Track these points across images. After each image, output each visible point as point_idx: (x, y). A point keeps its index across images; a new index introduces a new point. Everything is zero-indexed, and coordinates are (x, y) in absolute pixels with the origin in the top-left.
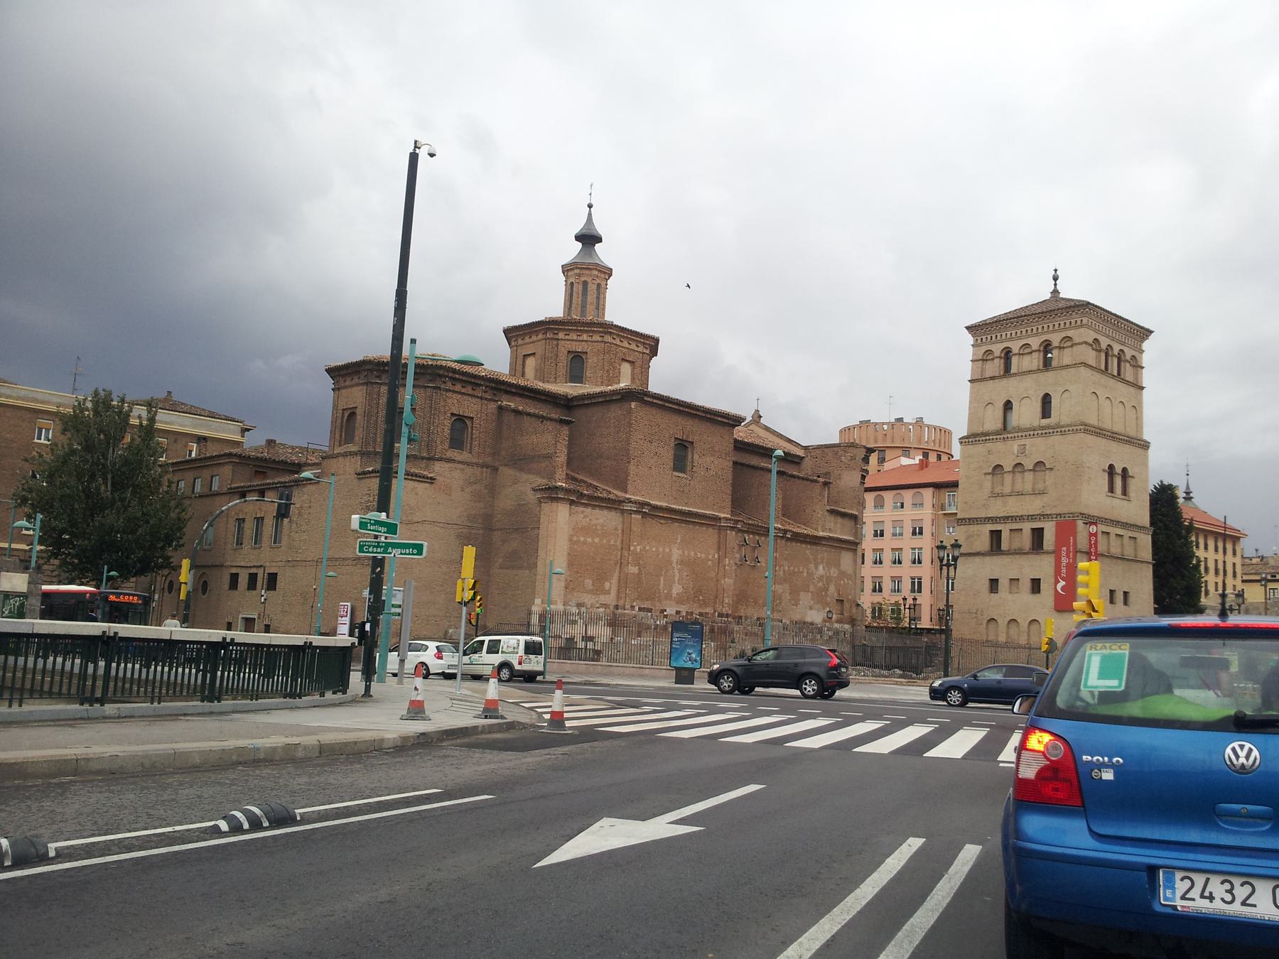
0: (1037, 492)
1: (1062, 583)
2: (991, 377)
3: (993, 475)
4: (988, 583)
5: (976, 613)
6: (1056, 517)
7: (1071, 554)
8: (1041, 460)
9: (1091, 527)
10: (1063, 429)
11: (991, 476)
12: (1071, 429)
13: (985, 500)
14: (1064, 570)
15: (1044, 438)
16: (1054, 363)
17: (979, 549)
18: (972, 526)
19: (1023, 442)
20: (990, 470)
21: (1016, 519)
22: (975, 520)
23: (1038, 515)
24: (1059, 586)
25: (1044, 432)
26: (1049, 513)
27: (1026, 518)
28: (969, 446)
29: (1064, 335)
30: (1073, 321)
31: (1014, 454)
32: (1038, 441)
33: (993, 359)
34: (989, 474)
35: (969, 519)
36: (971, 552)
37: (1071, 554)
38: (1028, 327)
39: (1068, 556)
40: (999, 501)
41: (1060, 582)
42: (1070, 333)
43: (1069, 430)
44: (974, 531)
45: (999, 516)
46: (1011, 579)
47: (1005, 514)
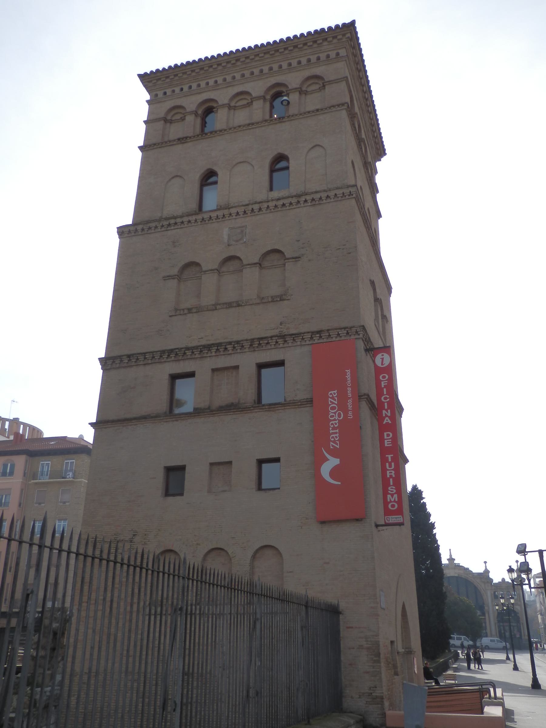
1: (333, 462)
2: (179, 139)
3: (179, 281)
4: (160, 475)
7: (350, 401)
8: (277, 247)
10: (317, 196)
11: (176, 280)
14: (335, 436)
16: (293, 110)
21: (226, 349)
24: (326, 470)
25: (280, 203)
27: (247, 345)
29: (307, 73)
33: (183, 119)
35: (129, 356)
36: (128, 416)
37: (350, 401)
39: (342, 406)
41: (327, 460)
42: (317, 71)
45: (190, 345)
46: (212, 464)
47: (204, 342)
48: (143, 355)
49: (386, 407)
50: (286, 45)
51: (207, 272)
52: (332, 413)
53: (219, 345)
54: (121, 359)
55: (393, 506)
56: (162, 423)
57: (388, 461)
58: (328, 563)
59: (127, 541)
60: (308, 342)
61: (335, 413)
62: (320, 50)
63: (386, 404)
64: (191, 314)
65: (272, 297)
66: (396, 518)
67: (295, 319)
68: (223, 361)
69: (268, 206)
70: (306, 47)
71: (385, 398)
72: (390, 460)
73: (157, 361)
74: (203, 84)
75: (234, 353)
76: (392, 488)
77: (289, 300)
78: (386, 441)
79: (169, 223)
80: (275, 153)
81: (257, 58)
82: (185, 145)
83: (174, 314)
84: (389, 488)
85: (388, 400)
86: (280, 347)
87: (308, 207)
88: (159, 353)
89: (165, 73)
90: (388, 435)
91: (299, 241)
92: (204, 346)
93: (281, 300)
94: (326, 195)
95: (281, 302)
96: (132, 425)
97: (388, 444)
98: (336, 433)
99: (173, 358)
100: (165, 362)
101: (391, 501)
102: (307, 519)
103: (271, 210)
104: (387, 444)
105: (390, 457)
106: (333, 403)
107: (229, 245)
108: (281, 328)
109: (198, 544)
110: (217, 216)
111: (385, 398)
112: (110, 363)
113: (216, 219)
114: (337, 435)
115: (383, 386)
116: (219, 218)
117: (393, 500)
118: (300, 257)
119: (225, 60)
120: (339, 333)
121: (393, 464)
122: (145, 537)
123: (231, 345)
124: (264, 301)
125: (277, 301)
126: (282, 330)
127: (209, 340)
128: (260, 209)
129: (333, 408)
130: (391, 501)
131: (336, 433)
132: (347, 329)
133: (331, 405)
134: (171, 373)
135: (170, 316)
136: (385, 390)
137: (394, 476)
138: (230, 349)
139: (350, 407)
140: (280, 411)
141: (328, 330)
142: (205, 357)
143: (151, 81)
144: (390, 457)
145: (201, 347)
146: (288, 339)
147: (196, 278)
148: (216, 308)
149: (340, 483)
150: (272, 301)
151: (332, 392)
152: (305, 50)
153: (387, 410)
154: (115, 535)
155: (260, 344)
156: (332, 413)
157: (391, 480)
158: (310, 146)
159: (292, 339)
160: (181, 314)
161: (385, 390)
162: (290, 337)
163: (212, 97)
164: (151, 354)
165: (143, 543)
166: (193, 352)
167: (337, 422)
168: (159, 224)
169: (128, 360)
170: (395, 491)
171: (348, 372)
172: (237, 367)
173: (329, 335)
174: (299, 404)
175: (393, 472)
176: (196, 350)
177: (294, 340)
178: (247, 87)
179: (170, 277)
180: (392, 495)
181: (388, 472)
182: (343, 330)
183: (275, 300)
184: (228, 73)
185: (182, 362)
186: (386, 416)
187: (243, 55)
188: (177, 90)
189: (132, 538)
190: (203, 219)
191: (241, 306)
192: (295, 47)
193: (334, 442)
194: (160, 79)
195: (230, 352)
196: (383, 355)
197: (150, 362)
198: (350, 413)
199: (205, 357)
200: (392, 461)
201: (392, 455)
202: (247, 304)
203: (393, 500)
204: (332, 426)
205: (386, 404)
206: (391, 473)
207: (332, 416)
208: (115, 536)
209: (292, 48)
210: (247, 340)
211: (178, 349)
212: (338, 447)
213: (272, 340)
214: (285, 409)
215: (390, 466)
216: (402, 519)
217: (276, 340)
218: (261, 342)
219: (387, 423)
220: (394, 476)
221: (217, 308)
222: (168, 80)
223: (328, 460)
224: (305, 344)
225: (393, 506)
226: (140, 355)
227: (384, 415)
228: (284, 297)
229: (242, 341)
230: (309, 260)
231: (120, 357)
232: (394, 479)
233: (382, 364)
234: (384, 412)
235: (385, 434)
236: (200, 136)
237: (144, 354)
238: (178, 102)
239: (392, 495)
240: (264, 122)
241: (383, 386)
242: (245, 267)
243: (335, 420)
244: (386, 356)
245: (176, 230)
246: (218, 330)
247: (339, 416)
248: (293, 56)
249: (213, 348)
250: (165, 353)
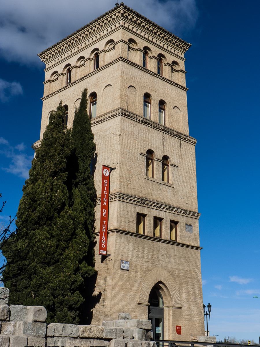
9: (105, 170)
49: (105, 197)
55: (103, 246)
71: (105, 192)
72: (104, 224)
84: (103, 237)
85: (106, 194)
90: (105, 211)
101: (103, 244)
104: (104, 215)
105: (104, 222)
111: (105, 192)
121: (105, 225)
130: (103, 244)
137: (105, 232)
144: (104, 222)
180: (104, 240)
181: (103, 229)
196: (106, 170)
206: (104, 230)
215: (104, 227)
216: (106, 253)
220: (105, 232)
225: (103, 246)
234: (104, 199)
235: (104, 210)
239: (104, 240)
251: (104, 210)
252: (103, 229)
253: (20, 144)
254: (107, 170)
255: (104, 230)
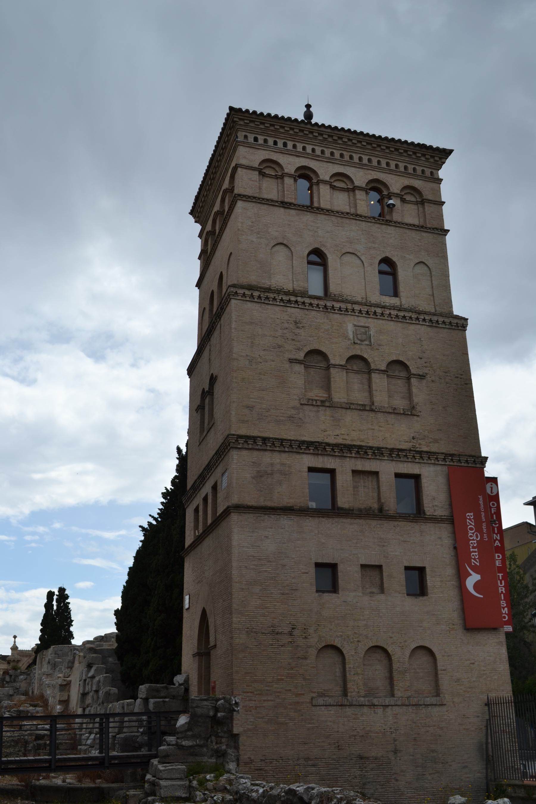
0: (402, 412)
5: (291, 634)
6: (444, 459)
8: (401, 359)
10: (435, 318)
12: (447, 320)
13: (293, 408)
14: (475, 554)
15: (400, 325)
16: (396, 217)
17: (286, 501)
18: (267, 453)
19: (363, 321)
20: (301, 356)
21: (366, 453)
22: (277, 444)
23: (410, 450)
25: (401, 314)
26: (425, 449)
28: (249, 305)
29: (407, 182)
30: (419, 169)
31: (346, 337)
32: (391, 326)
34: (299, 362)
36: (269, 504)
38: (345, 150)
39: (478, 529)
40: (325, 415)
43: (444, 322)
44: (272, 464)
46: (363, 566)
47: (340, 441)
48: (280, 441)
49: (496, 532)
50: (389, 144)
51: (336, 367)
52: (471, 533)
53: (360, 447)
54: (255, 440)
56: (307, 517)
57: (499, 579)
58: (473, 664)
59: (286, 633)
60: (440, 463)
61: (473, 533)
62: (417, 163)
63: (496, 529)
64: (324, 408)
65: (403, 410)
66: (507, 628)
67: (425, 436)
68: (361, 465)
69: (390, 313)
70: (405, 154)
71: (496, 524)
72: (501, 578)
73: (295, 450)
74: (300, 147)
75: (373, 459)
76: (503, 602)
77: (418, 416)
78: (497, 561)
79: (289, 299)
80: (383, 256)
81: (359, 145)
82: (287, 210)
83: (306, 403)
85: (497, 525)
86: (417, 461)
87: (426, 326)
88: (297, 442)
89: (261, 118)
90: (499, 557)
91: (421, 358)
92: (345, 446)
93: (411, 415)
94: (442, 320)
95: (411, 417)
96: (275, 514)
97: (499, 564)
98: (475, 552)
99: (311, 451)
100: (303, 453)
102: (453, 625)
103: (392, 318)
106: (471, 524)
107: (354, 343)
108: (414, 443)
109: (358, 641)
110: (340, 308)
112: (242, 442)
113: (338, 310)
114: (477, 554)
115: (493, 513)
116: (342, 311)
117: (504, 612)
118: (425, 376)
119: (328, 132)
120: (468, 459)
121: (503, 581)
122: (305, 631)
123: (372, 450)
124: (396, 411)
125: (408, 414)
126: (414, 444)
127: (346, 440)
128: (382, 314)
129: (471, 529)
131: (475, 552)
132: (474, 458)
133: (469, 526)
134: (310, 466)
135: (301, 404)
136: (494, 516)
137: (504, 592)
138: (370, 453)
139: (485, 530)
140: (422, 523)
141: (459, 455)
142: (345, 457)
143: (243, 120)
145: (342, 446)
146: (425, 456)
147: (319, 368)
148: (350, 407)
149: (482, 596)
150: (403, 414)
151: (469, 514)
152: (404, 156)
153: (497, 534)
154: (272, 627)
155: (398, 455)
156: (471, 533)
157: (502, 595)
158: (417, 262)
159: (428, 456)
160: (312, 405)
161: (494, 516)
162: (426, 454)
163: (311, 166)
164: (289, 442)
165: (304, 637)
166: (333, 449)
167: (475, 542)
168: (279, 297)
169: (262, 443)
170: (505, 605)
171: (481, 497)
172: (376, 474)
173: (460, 460)
174: (440, 520)
175: (504, 589)
176: (336, 448)
177: (429, 458)
178: (349, 171)
179: (297, 361)
180: (504, 608)
181: (500, 588)
182: (471, 458)
183: (406, 413)
184: (327, 146)
185: (320, 457)
186: (497, 539)
187: (346, 136)
188: (271, 141)
189: (291, 631)
190: (325, 306)
191: (374, 411)
192: (397, 150)
193: (475, 559)
194: (254, 122)
195: (370, 457)
196: (492, 484)
197: (287, 449)
198: (485, 536)
199: (345, 457)
200: (502, 579)
201: (502, 574)
202: (381, 410)
203: (504, 612)
204: (472, 545)
205: (496, 529)
206: (502, 589)
207: (471, 536)
208: (272, 628)
209: (393, 150)
210: (387, 448)
211: (318, 442)
212: (478, 564)
213: (410, 453)
214: (426, 522)
215: (501, 584)
217: (414, 454)
218: (400, 453)
219: (497, 546)
220: (504, 592)
221: (351, 408)
222: (262, 126)
223: (471, 575)
224: (438, 463)
226: (277, 441)
227: (495, 539)
228: (414, 412)
229: (383, 448)
230: (433, 381)
231: (254, 439)
232: (504, 594)
233: (492, 493)
236: (306, 208)
237: (282, 440)
238: (275, 157)
240: (372, 219)
241: (493, 513)
242: (374, 371)
243: (473, 540)
244: (494, 485)
245: (296, 309)
246: (353, 430)
247: (477, 537)
248: (392, 158)
249: (354, 449)
250: (304, 444)
251: (497, 555)
252: (500, 588)
253: (117, 629)
254: (493, 484)
255: (503, 590)
